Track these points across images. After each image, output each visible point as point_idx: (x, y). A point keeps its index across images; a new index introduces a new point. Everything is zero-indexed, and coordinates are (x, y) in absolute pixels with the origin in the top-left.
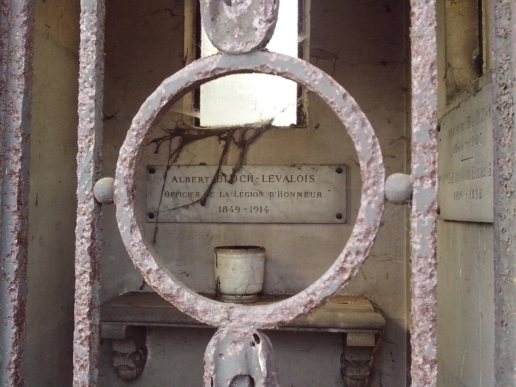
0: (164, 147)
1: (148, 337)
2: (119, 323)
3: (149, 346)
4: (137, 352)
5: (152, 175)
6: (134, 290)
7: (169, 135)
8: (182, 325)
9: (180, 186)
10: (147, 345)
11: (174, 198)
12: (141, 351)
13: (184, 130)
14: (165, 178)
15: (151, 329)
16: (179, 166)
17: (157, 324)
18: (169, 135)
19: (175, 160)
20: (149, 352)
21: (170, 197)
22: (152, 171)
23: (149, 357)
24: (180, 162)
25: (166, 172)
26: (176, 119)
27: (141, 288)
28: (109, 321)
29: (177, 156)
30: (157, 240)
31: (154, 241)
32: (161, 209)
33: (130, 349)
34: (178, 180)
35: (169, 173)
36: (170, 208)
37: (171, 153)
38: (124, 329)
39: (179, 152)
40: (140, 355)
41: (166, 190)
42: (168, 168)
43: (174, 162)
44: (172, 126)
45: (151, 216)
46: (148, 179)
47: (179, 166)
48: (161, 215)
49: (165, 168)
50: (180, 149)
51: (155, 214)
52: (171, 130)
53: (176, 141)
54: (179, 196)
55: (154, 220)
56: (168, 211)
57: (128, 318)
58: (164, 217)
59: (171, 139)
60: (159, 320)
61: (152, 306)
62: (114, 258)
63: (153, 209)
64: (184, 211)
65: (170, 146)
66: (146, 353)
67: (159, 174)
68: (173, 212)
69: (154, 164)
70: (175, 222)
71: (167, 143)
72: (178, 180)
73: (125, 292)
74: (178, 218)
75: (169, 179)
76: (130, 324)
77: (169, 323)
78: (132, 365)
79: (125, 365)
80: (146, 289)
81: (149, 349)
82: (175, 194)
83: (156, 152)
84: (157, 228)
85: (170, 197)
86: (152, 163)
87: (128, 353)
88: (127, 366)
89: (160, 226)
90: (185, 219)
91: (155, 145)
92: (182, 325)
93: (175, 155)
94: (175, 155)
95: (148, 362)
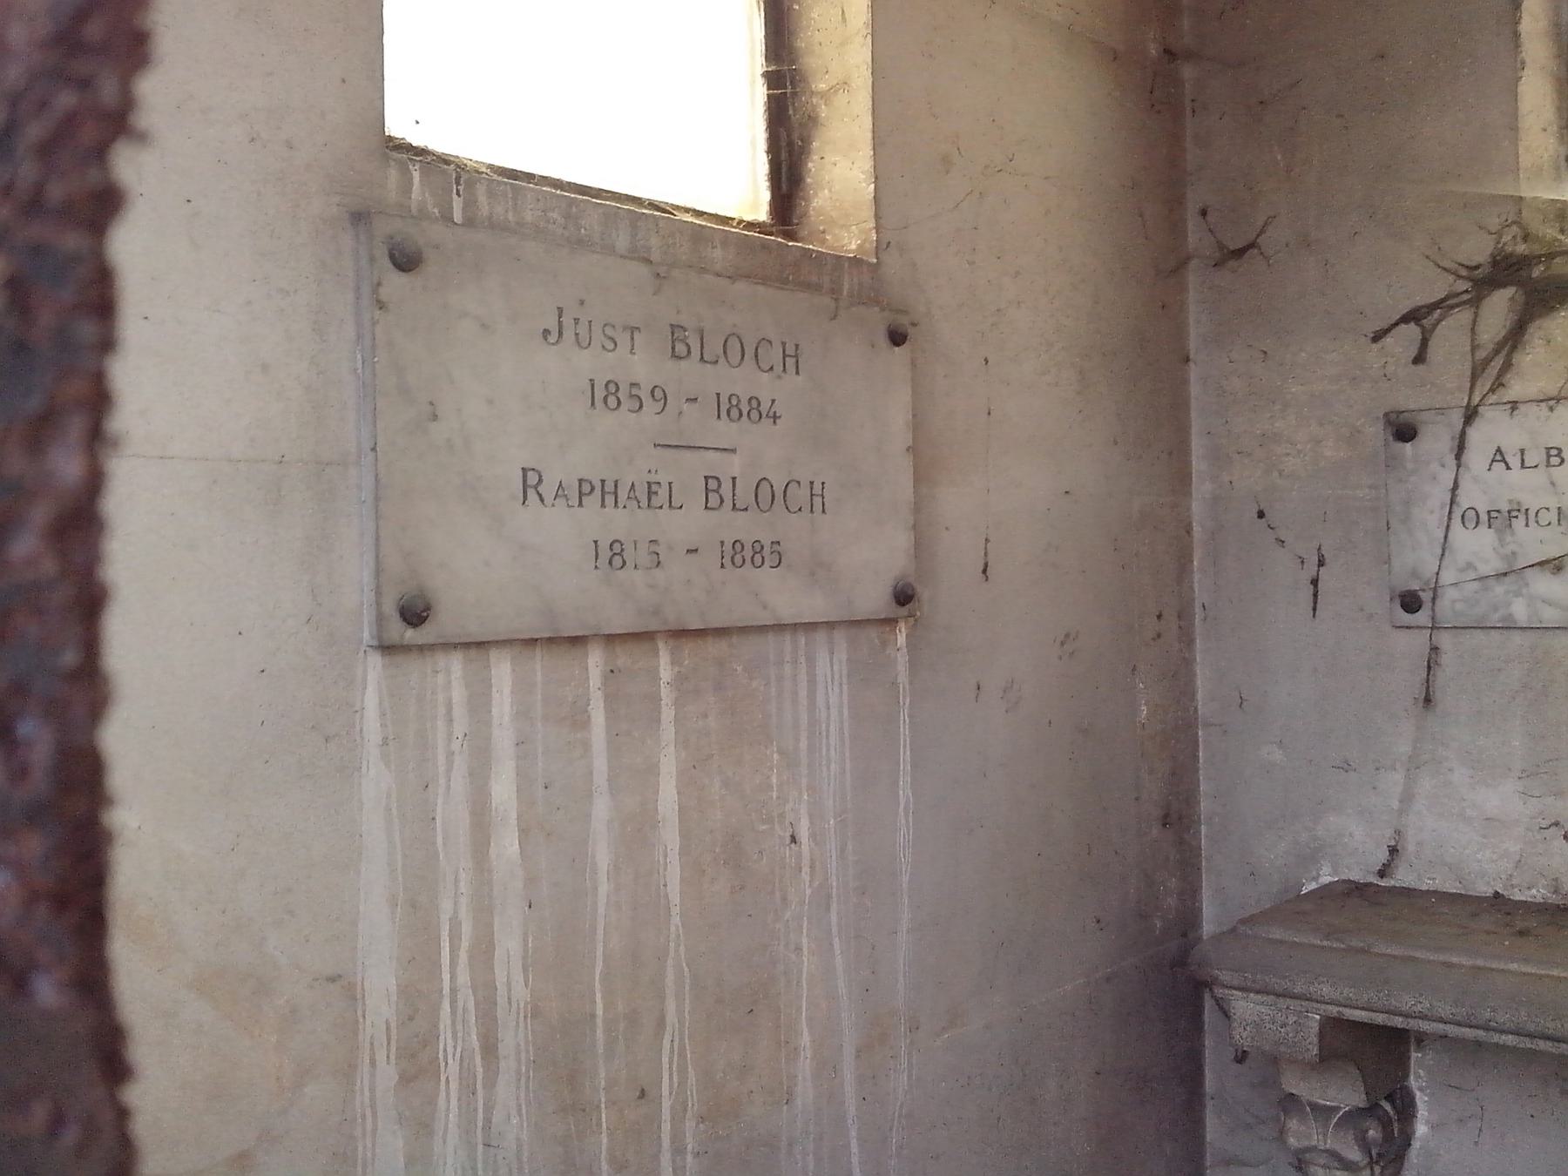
0: (1451, 335)
1: (1415, 1055)
2: (1291, 1003)
3: (1421, 1089)
4: (1372, 1110)
5: (1408, 445)
6: (1356, 875)
7: (1463, 285)
8: (1543, 1045)
9: (1524, 486)
10: (1413, 1083)
11: (1499, 532)
12: (1388, 1107)
13: (1526, 262)
14: (1458, 457)
15: (1421, 1039)
16: (1514, 405)
17: (1441, 1026)
18: (1463, 285)
19: (1498, 384)
20: (1422, 1111)
21: (1483, 528)
22: (1405, 432)
23: (1421, 1129)
24: (1517, 388)
25: (1463, 434)
26: (1494, 223)
27: (1382, 874)
28: (1258, 992)
29: (1507, 366)
30: (1438, 695)
31: (1428, 700)
32: (1447, 577)
33: (1345, 1094)
34: (1514, 462)
35: (1473, 434)
36: (1485, 569)
37: (1481, 354)
38: (1315, 1027)
39: (1514, 347)
40: (1386, 1124)
41: (1464, 501)
42: (1471, 415)
43: (1492, 391)
44: (1477, 250)
45: (1410, 602)
46: (1392, 463)
47: (1514, 405)
48: (1449, 597)
49: (1457, 418)
50: (1515, 336)
51: (1426, 597)
52: (1477, 267)
53: (1499, 307)
54: (1519, 524)
55: (1422, 617)
56: (1476, 585)
57: (1326, 990)
58: (1459, 606)
59: (1476, 302)
60: (1445, 1010)
61: (1418, 954)
62: (1278, 756)
63: (1415, 574)
64: (1544, 584)
65: (1473, 329)
66: (1407, 1111)
67: (1435, 441)
68: (1499, 589)
69: (1412, 407)
70: (1509, 627)
71: (1463, 316)
72: (1514, 462)
73: (1326, 880)
74: (1520, 611)
75: (1477, 456)
76: (1333, 1010)
77: (1487, 1029)
78: (1354, 1154)
79: (1326, 1151)
80: (1403, 877)
81: (1421, 1100)
82: (1503, 518)
83: (1419, 359)
84: (1435, 649)
85: (1483, 528)
86: (1407, 400)
87: (1337, 1109)
88: (1333, 1154)
89: (1445, 640)
90: (1550, 616)
91: (1411, 331)
92: (1543, 1045)
93: (1498, 362)
94: (1498, 362)
95: (1416, 1144)
